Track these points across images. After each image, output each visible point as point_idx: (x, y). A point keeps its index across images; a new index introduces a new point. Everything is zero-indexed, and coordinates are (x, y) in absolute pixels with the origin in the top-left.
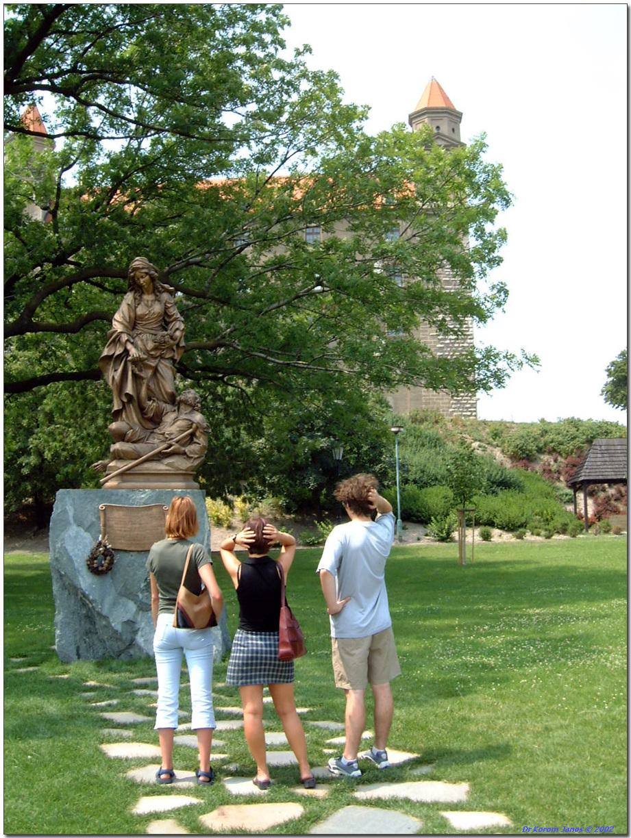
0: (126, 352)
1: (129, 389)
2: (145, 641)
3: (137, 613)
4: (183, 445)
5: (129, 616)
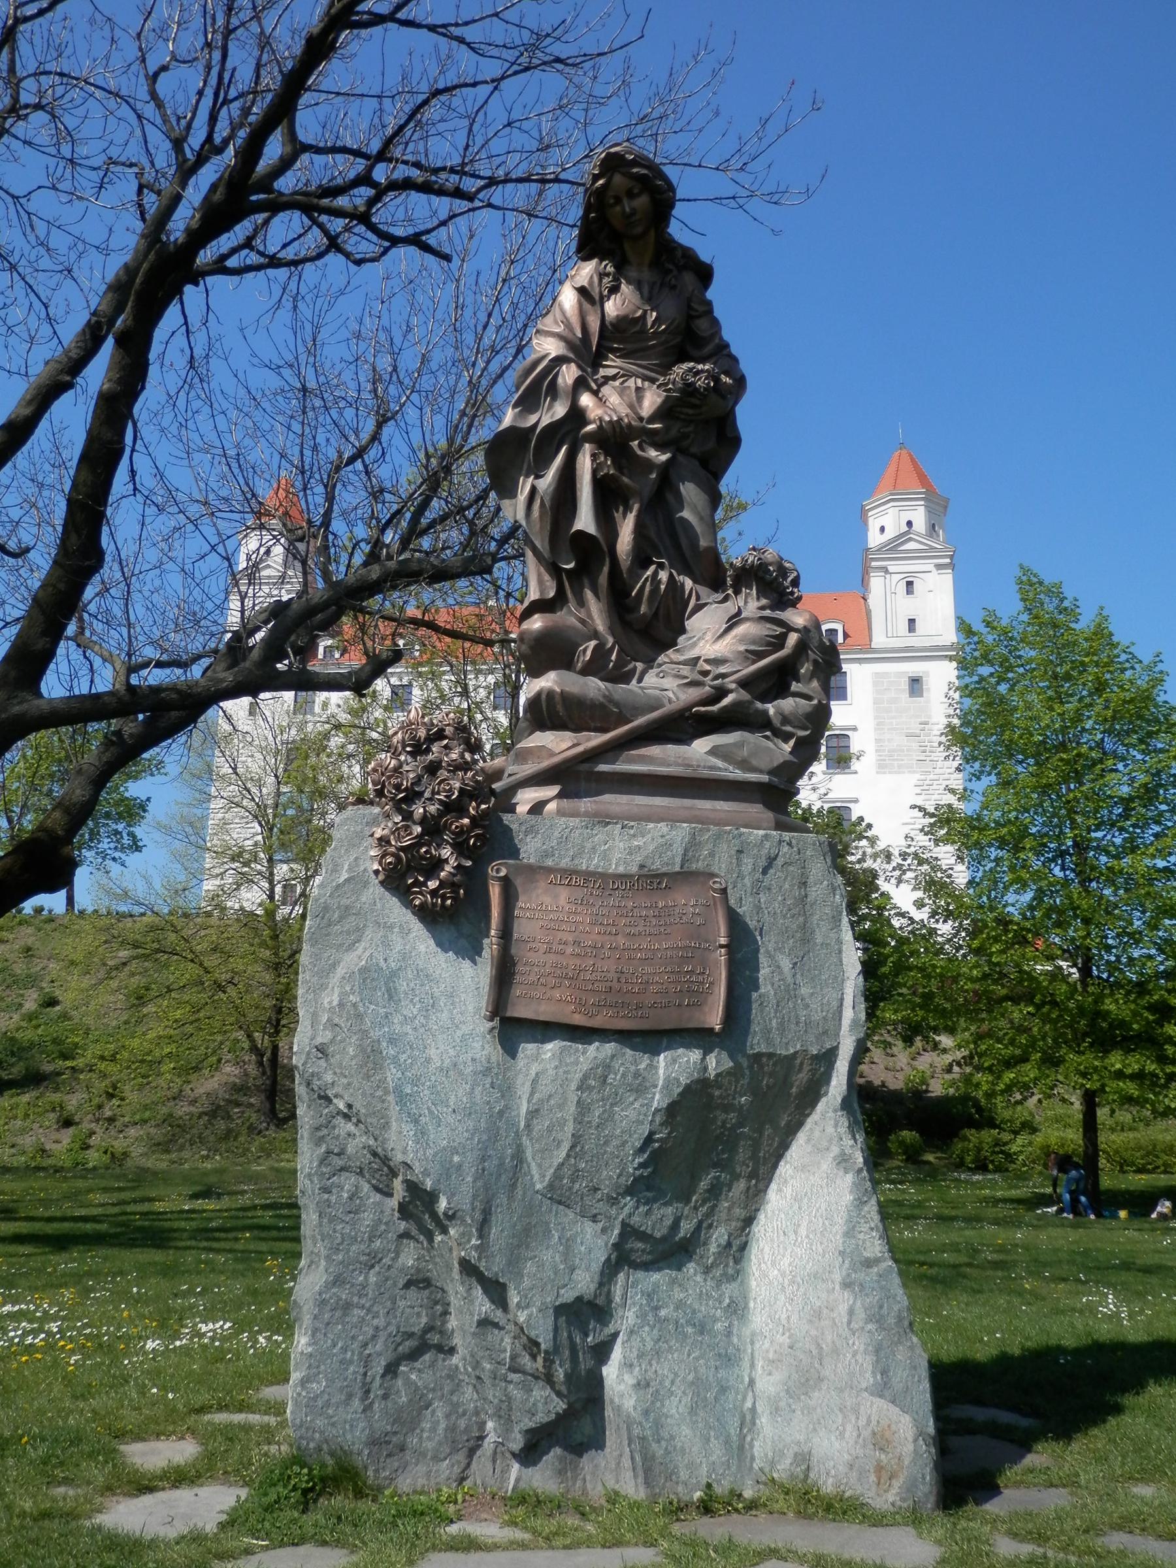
0: (577, 415)
1: (585, 520)
2: (638, 1385)
3: (610, 1271)
4: (766, 698)
5: (584, 1283)
